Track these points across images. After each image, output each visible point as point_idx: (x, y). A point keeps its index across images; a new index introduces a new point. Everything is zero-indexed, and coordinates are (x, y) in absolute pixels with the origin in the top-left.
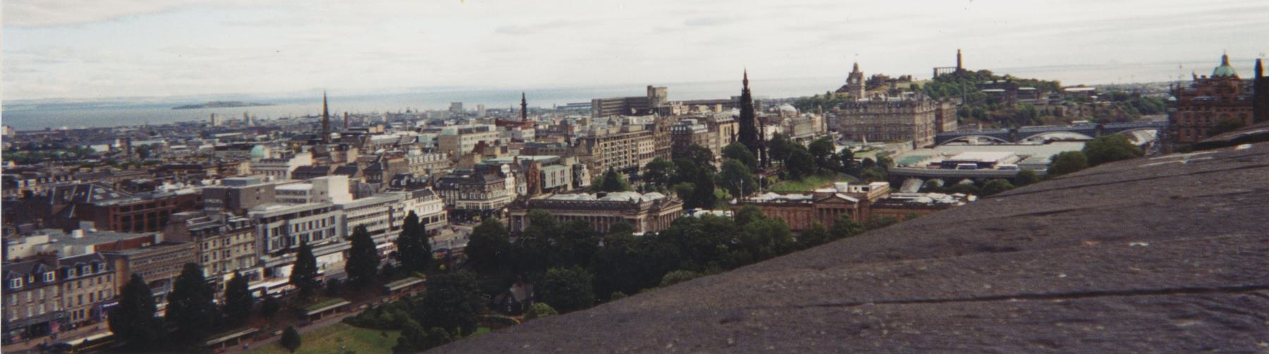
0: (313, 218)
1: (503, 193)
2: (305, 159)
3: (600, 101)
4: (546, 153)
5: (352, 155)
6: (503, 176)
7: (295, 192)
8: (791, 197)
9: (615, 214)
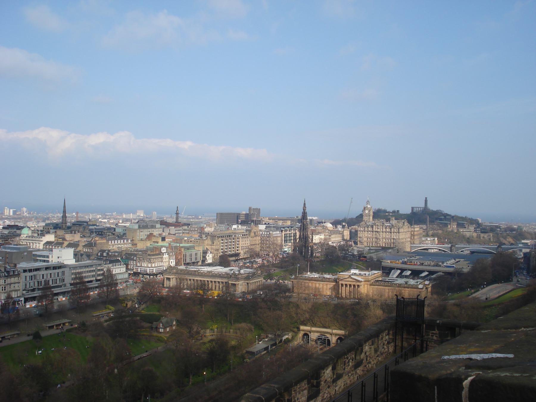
1: (161, 264)
3: (222, 214)
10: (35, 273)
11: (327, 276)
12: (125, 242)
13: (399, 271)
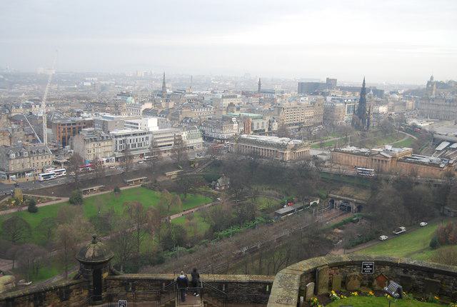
0: (138, 137)
2: (149, 106)
4: (259, 112)
5: (171, 105)
6: (232, 122)
7: (135, 124)
8: (363, 150)
9: (275, 149)
10: (124, 138)
11: (363, 150)
13: (448, 143)
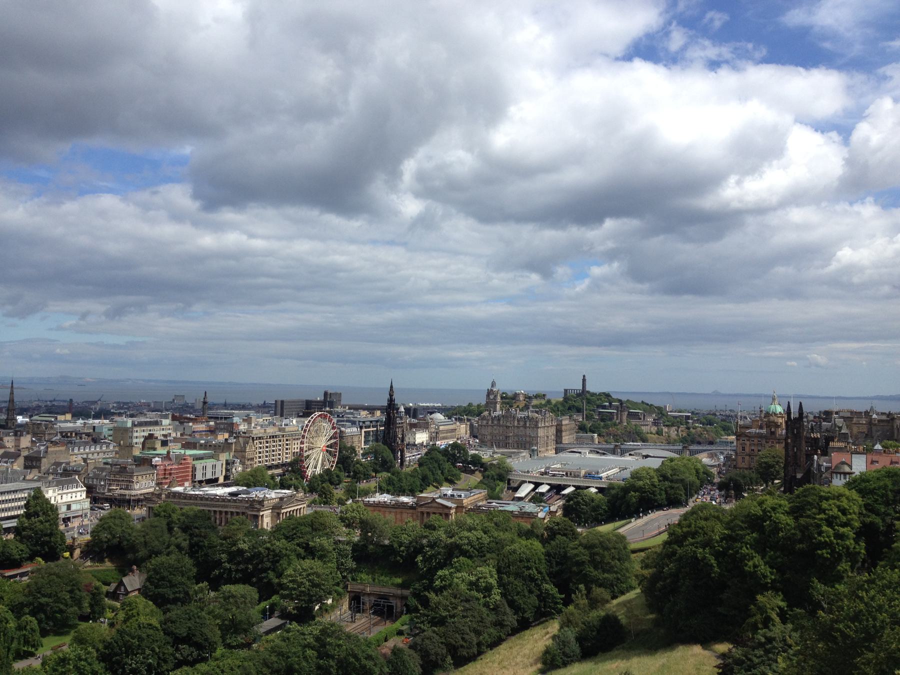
3: (282, 402)
4: (203, 447)
5: (26, 441)
8: (404, 499)
11: (404, 499)
12: (104, 448)
13: (532, 486)
